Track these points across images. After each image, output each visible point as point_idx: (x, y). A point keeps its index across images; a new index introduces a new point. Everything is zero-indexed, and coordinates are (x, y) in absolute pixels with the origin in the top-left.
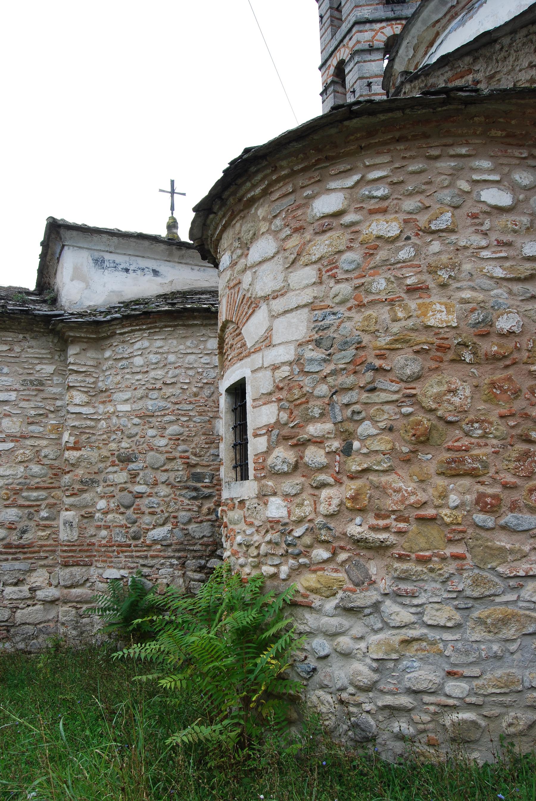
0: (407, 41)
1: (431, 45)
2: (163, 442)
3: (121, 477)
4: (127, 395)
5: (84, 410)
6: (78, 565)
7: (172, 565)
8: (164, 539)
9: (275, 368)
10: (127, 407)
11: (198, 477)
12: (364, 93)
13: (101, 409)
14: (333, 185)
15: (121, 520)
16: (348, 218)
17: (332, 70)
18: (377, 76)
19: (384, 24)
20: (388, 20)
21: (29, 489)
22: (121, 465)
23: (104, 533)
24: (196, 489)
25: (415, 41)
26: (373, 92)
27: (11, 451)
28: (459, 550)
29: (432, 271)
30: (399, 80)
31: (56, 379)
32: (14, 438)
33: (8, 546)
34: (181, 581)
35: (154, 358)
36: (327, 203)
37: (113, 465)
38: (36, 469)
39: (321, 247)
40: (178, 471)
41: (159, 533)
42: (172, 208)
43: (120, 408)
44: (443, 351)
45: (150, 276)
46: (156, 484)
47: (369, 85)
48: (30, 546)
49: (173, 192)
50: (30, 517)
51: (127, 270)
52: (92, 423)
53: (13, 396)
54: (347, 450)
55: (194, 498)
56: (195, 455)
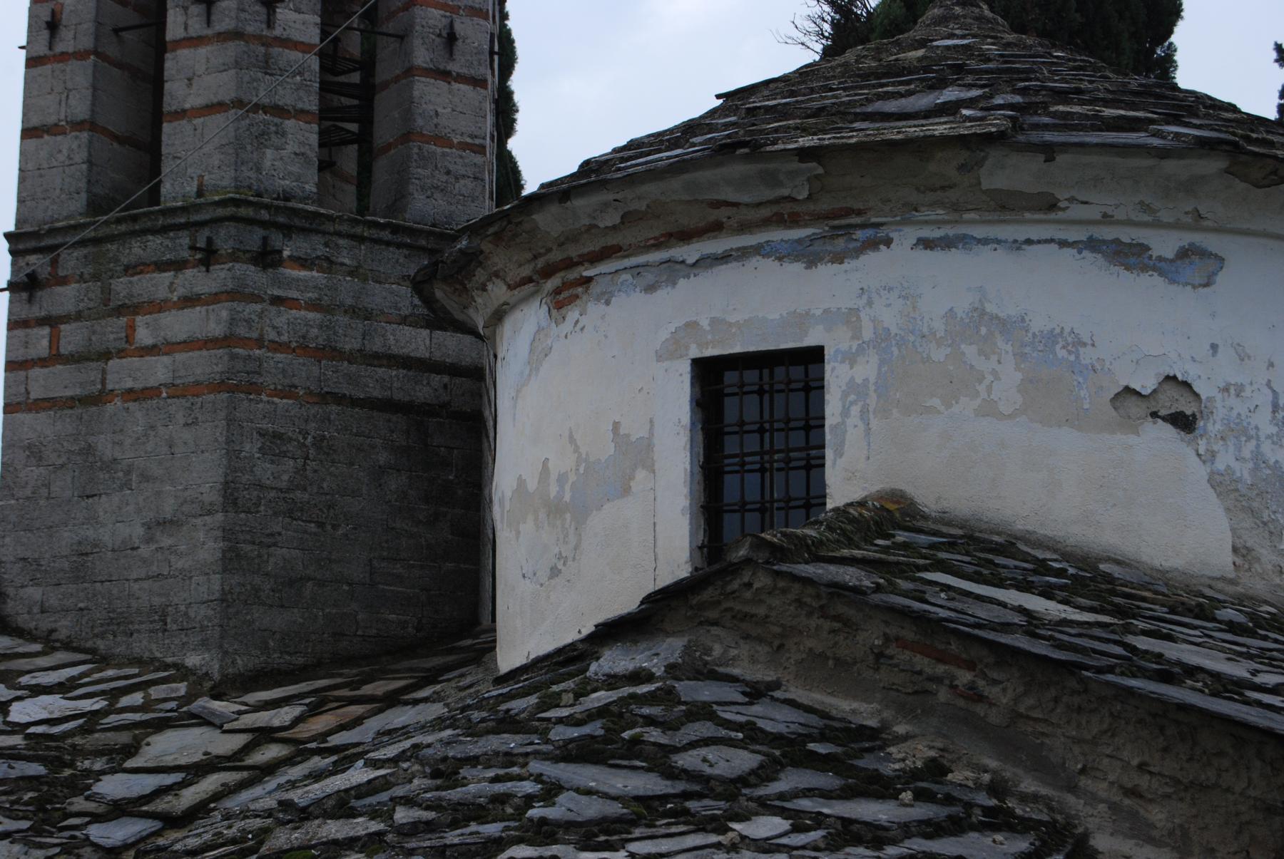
0: (618, 196)
1: (685, 236)
12: (250, 29)
25: (642, 206)
26: (278, 32)
30: (742, 552)
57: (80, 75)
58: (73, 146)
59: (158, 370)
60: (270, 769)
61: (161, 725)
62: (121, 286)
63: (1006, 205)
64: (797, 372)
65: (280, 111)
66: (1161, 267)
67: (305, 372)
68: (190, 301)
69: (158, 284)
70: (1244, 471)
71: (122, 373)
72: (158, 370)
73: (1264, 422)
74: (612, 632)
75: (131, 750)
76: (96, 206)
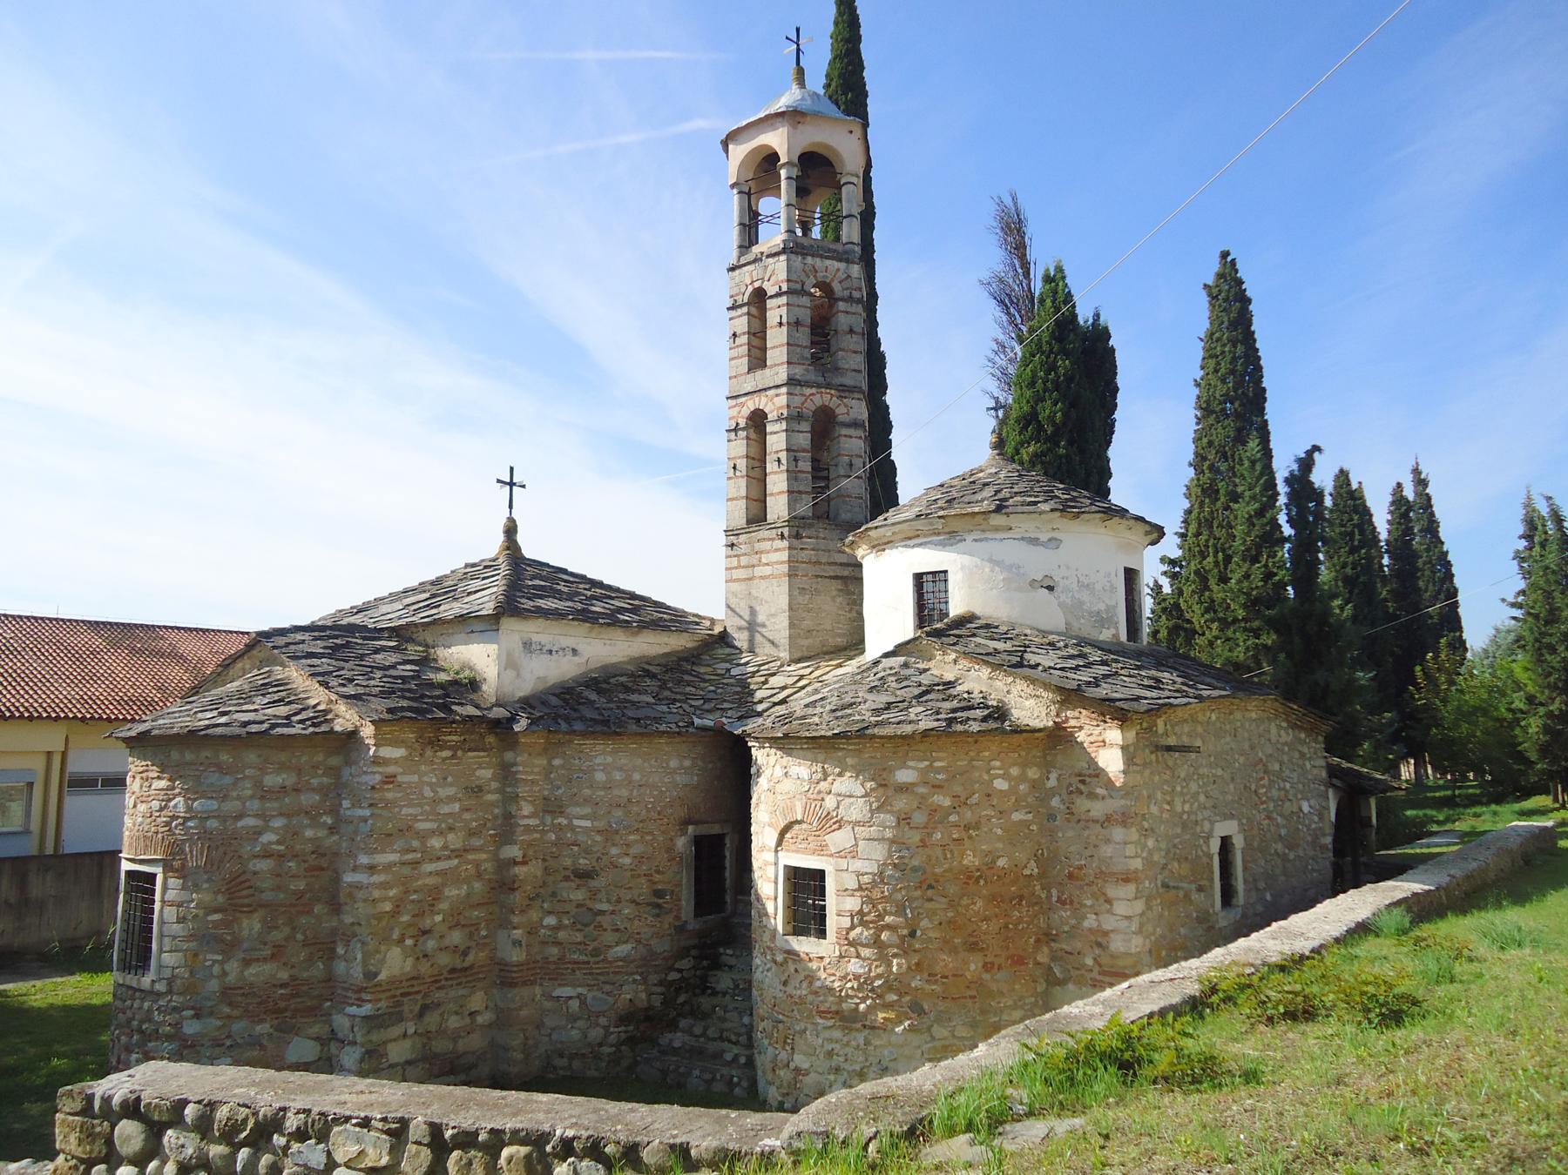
2: (627, 861)
3: (579, 895)
4: (587, 810)
5: (532, 822)
6: (525, 983)
7: (635, 981)
8: (628, 955)
9: (859, 874)
10: (588, 824)
11: (658, 894)
13: (548, 819)
14: (911, 763)
15: (579, 937)
16: (922, 790)
17: (746, 412)
18: (804, 451)
19: (814, 390)
20: (819, 386)
21: (472, 907)
22: (578, 881)
23: (555, 950)
24: (658, 906)
27: (457, 867)
28: (974, 993)
29: (967, 828)
31: (494, 785)
32: (458, 853)
33: (453, 970)
34: (643, 996)
35: (618, 776)
36: (905, 776)
37: (567, 878)
38: (477, 885)
39: (901, 803)
40: (643, 889)
41: (623, 949)
42: (511, 507)
43: (576, 822)
44: (970, 878)
45: (569, 656)
46: (619, 901)
47: (796, 460)
48: (471, 967)
49: (511, 484)
50: (471, 935)
51: (550, 652)
52: (537, 835)
53: (457, 807)
54: (912, 934)
55: (658, 916)
56: (658, 872)
57: (743, 482)
58: (742, 504)
59: (767, 570)
60: (803, 688)
61: (774, 674)
62: (758, 546)
63: (997, 529)
64: (928, 587)
65: (800, 492)
66: (1043, 544)
67: (812, 570)
68: (777, 550)
69: (767, 545)
70: (1069, 601)
71: (759, 571)
72: (767, 570)
73: (1075, 586)
74: (887, 655)
75: (766, 682)
76: (749, 522)
